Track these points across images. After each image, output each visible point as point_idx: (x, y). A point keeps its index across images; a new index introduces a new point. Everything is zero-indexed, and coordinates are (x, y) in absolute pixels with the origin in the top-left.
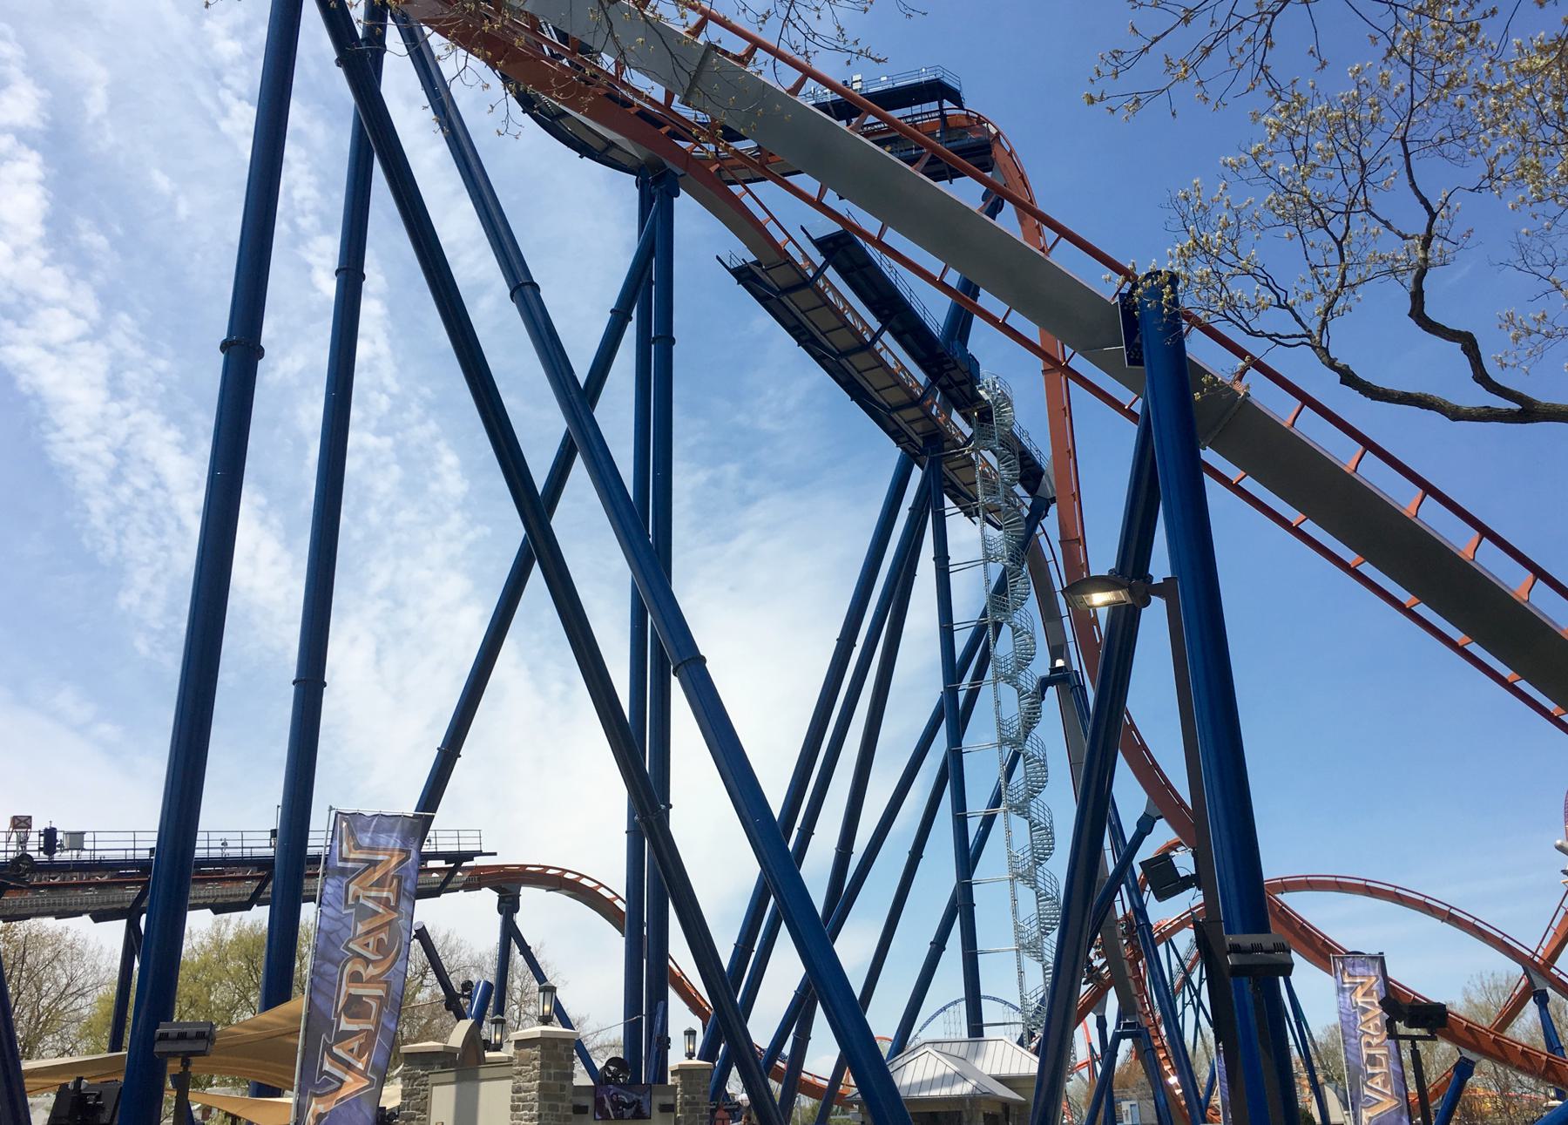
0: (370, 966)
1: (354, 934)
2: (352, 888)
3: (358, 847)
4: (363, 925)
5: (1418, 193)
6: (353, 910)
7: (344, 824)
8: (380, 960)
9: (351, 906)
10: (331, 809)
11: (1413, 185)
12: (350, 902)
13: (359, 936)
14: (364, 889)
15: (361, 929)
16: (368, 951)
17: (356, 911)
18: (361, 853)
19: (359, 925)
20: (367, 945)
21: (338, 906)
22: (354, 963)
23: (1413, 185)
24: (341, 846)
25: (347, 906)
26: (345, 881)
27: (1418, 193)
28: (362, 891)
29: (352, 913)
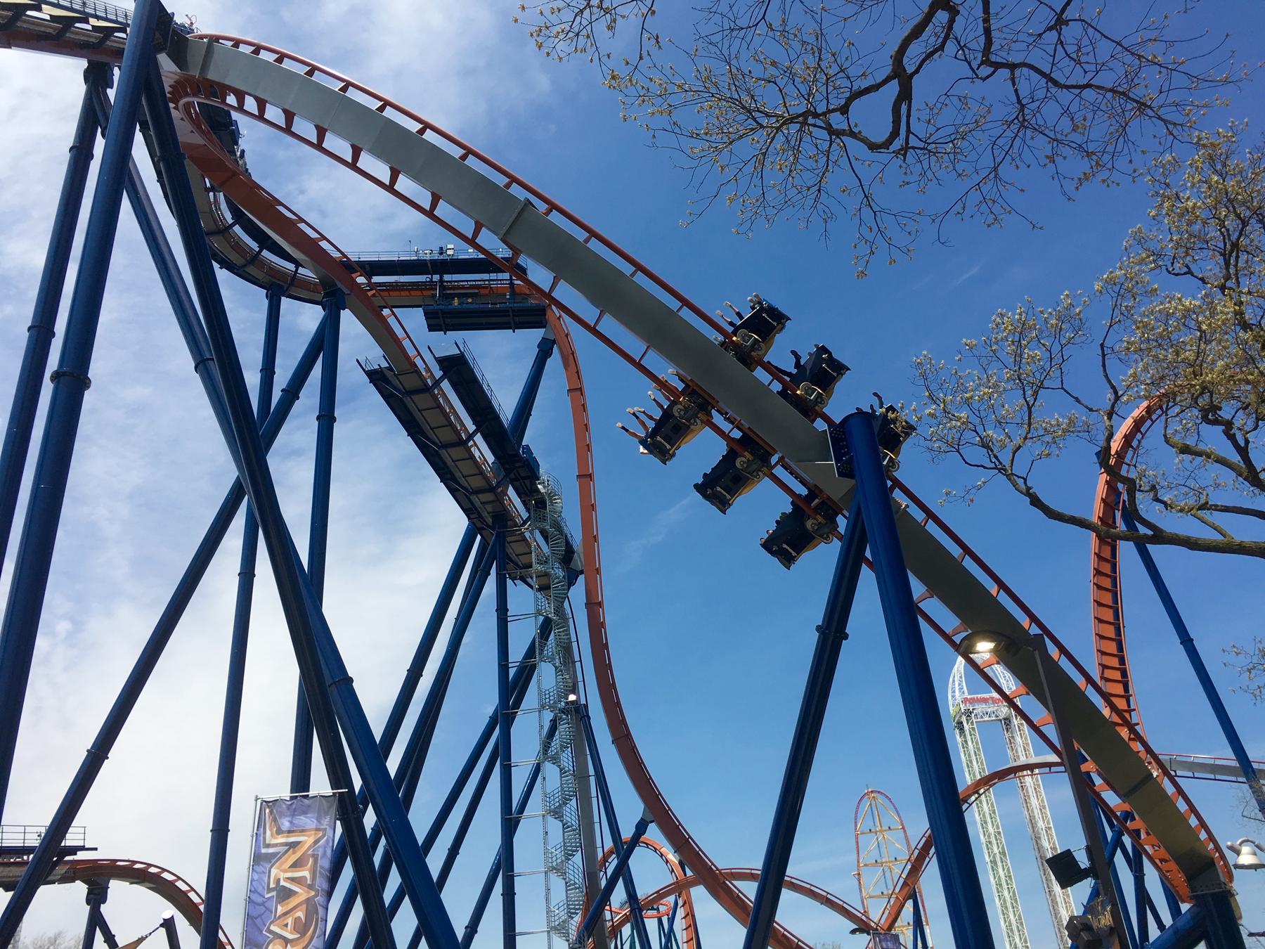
0: (289, 945)
1: (275, 916)
2: (274, 871)
3: (279, 832)
4: (282, 906)
5: (1109, 382)
6: (274, 893)
7: (267, 811)
8: (298, 939)
9: (273, 890)
10: (257, 799)
11: (1106, 376)
12: (272, 885)
13: (280, 917)
14: (281, 870)
15: (280, 910)
16: (287, 931)
17: (277, 893)
18: (283, 837)
19: (279, 907)
20: (286, 925)
21: (260, 890)
22: (274, 945)
23: (1106, 376)
24: (265, 833)
25: (270, 890)
26: (268, 866)
27: (1109, 382)
28: (282, 873)
29: (273, 896)
